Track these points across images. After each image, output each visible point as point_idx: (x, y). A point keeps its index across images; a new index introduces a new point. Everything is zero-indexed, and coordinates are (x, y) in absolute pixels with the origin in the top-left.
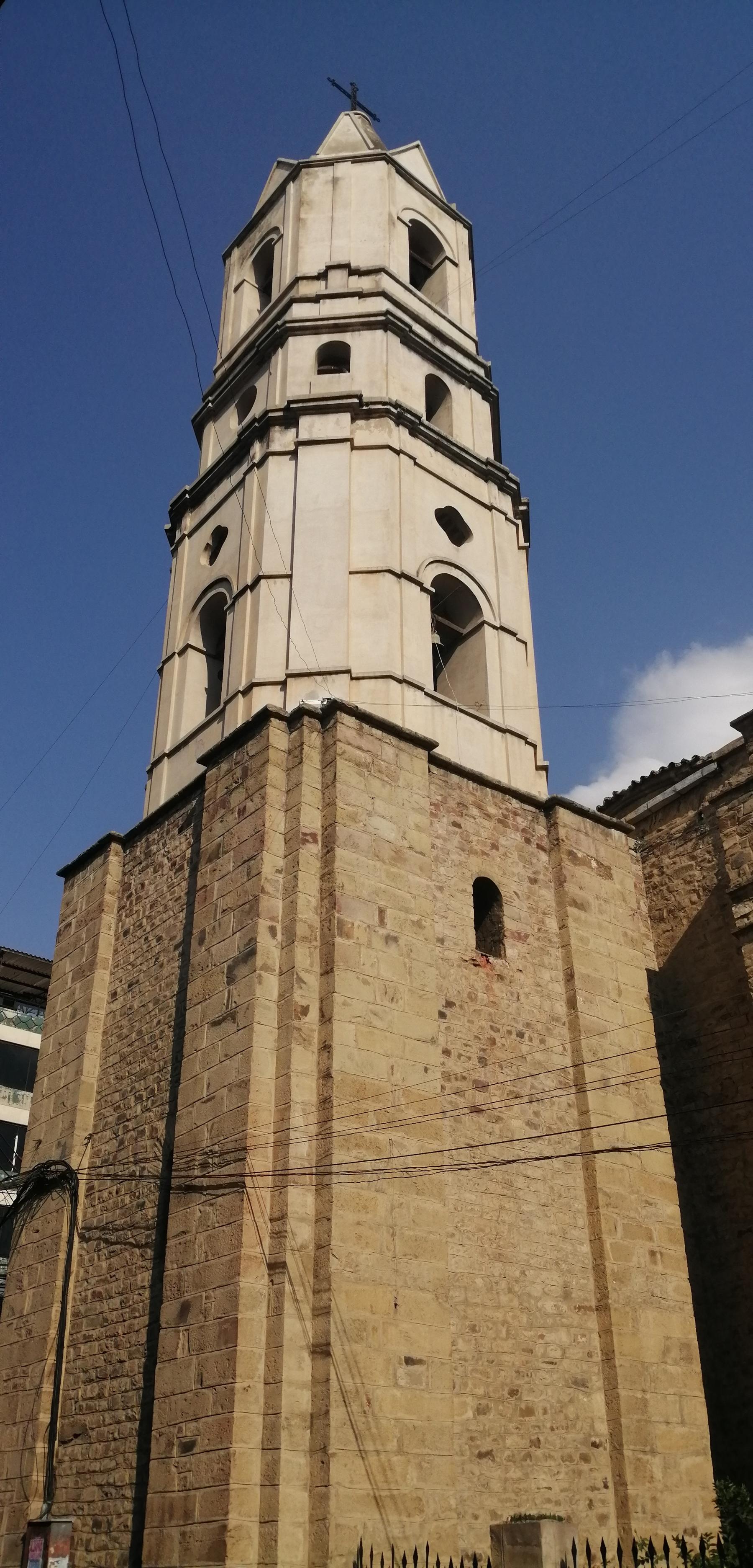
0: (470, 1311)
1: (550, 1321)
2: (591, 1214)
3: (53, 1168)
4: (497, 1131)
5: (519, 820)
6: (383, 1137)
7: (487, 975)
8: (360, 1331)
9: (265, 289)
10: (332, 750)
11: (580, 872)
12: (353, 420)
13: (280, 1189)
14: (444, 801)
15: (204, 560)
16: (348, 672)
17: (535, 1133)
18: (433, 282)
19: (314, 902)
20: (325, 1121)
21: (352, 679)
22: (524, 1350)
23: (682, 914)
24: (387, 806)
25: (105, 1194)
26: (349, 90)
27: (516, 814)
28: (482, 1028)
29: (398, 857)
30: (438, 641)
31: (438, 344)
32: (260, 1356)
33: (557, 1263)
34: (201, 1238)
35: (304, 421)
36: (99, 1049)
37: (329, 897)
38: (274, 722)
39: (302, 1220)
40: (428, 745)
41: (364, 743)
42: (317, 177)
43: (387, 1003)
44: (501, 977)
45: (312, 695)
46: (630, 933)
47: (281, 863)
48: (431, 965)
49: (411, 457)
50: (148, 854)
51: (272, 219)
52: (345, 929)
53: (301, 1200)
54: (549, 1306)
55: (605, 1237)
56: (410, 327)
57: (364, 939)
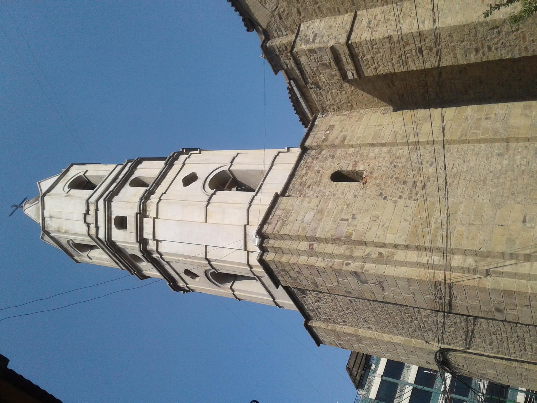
0: (506, 195)
1: (512, 162)
2: (469, 143)
3: (438, 358)
4: (433, 179)
5: (308, 161)
6: (433, 226)
7: (370, 178)
8: (511, 241)
9: (91, 247)
10: (276, 235)
11: (331, 138)
12: (145, 217)
13: (452, 269)
14: (299, 191)
17: (435, 164)
18: (93, 181)
20: (425, 249)
21: (248, 224)
22: (523, 173)
23: (350, 98)
24: (300, 213)
25: (450, 338)
26: (14, 208)
27: (306, 162)
28: (391, 182)
29: (321, 212)
30: (235, 189)
31: (118, 180)
32: (519, 282)
33: (488, 158)
34: (470, 302)
35: (145, 236)
36: (391, 336)
37: (336, 241)
38: (264, 258)
39: (465, 261)
41: (274, 222)
43: (379, 221)
44: (371, 173)
45: (254, 242)
46: (356, 119)
48: (365, 201)
49: (162, 195)
50: (313, 310)
51: (64, 243)
52: (348, 235)
53: (457, 261)
54: (505, 162)
55: (479, 138)
56: (110, 192)
57: (353, 228)
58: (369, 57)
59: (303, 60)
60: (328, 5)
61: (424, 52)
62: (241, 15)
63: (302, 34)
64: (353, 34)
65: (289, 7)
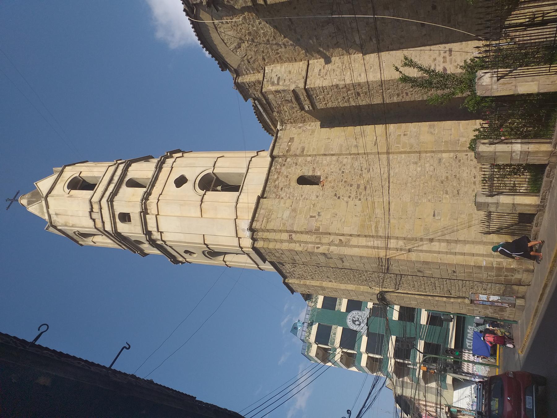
0: (421, 194)
1: (423, 169)
5: (278, 167)
11: (293, 148)
12: (148, 214)
14: (275, 193)
15: (195, 256)
16: (235, 219)
19: (309, 236)
27: (276, 168)
29: (294, 210)
34: (401, 267)
35: (150, 229)
39: (397, 243)
40: (259, 198)
41: (261, 220)
42: (55, 220)
47: (298, 244)
51: (70, 233)
54: (419, 169)
57: (320, 223)
58: (321, 97)
59: (271, 97)
60: (287, 55)
61: (361, 95)
62: (216, 60)
63: (267, 76)
64: (308, 80)
65: (255, 55)
